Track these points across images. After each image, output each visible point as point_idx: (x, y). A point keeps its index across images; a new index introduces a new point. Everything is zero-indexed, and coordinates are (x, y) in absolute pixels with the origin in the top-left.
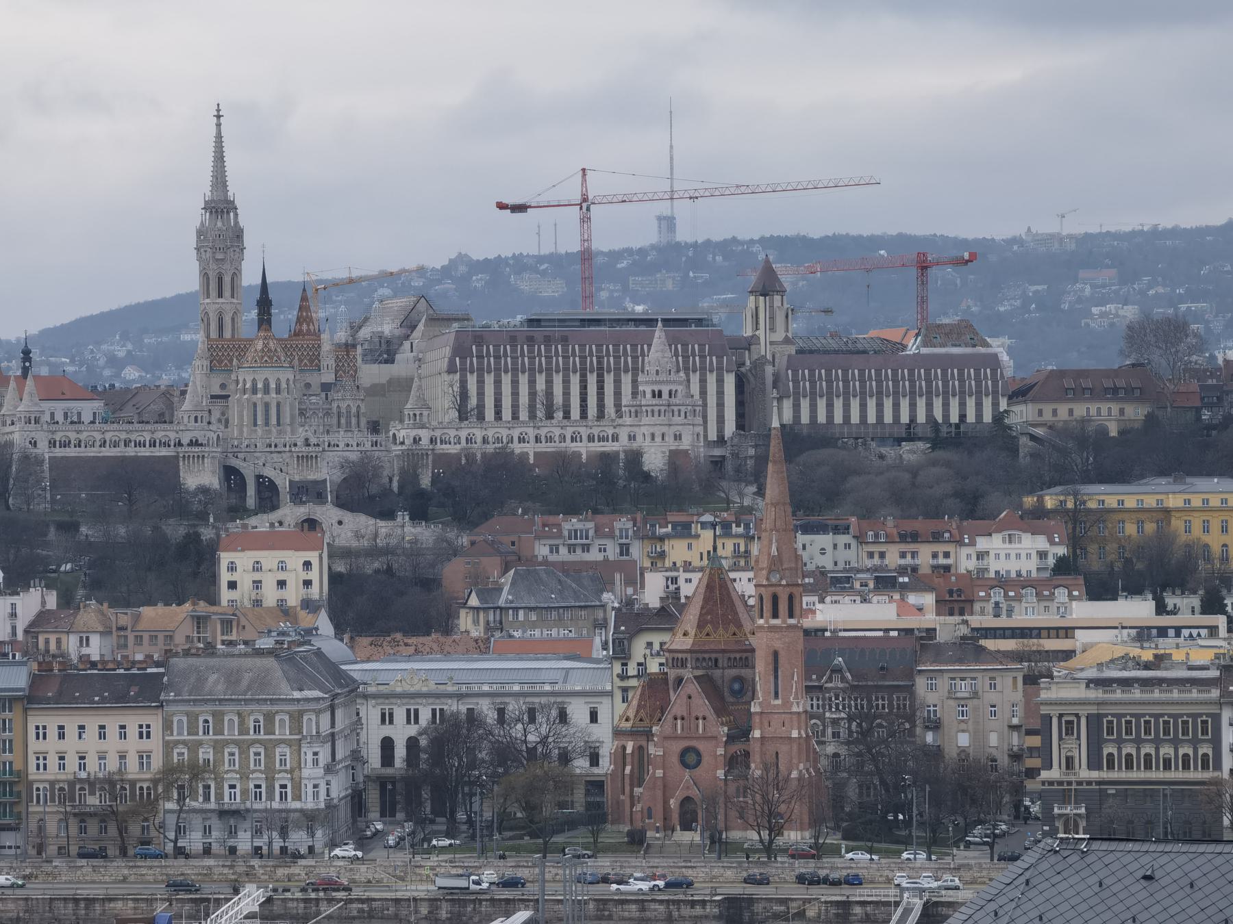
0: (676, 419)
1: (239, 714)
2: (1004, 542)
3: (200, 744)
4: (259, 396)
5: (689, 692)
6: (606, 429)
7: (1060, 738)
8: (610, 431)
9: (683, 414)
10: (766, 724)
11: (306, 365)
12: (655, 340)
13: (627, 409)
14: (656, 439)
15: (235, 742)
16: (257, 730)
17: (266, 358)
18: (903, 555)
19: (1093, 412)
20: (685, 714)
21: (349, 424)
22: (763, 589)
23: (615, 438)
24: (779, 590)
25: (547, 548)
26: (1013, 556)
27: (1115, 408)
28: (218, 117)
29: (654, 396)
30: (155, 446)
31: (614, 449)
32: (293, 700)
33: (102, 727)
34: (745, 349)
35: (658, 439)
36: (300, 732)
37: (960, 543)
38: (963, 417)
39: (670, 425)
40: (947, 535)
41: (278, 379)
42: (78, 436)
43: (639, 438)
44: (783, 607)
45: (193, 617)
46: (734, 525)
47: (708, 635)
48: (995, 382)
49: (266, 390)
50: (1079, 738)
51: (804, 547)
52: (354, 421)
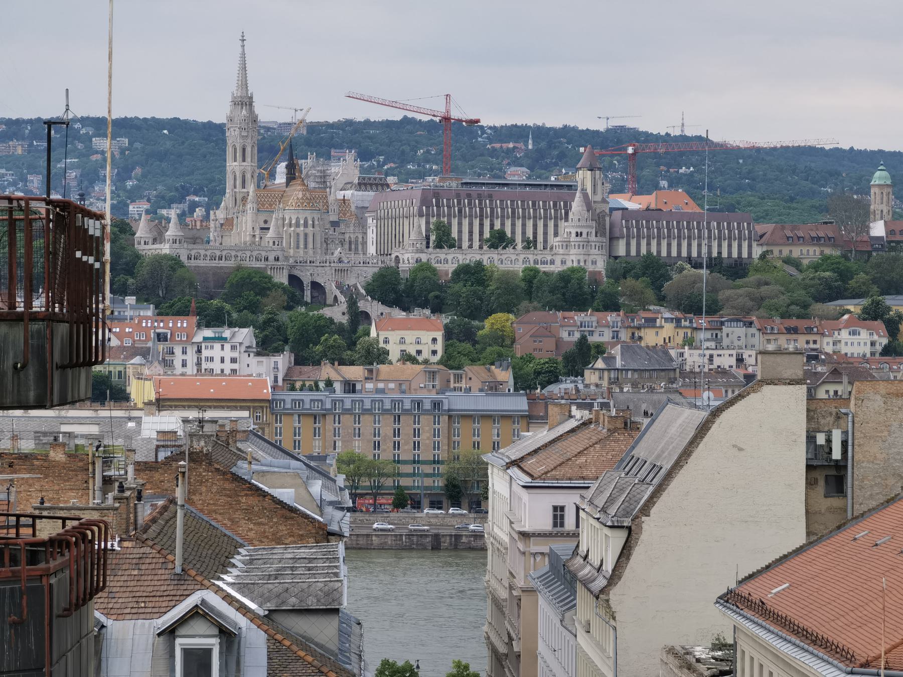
2: (850, 334)
6: (546, 256)
8: (549, 258)
9: (597, 247)
13: (557, 244)
17: (305, 204)
18: (808, 342)
23: (552, 262)
25: (567, 332)
26: (856, 344)
27: (818, 250)
29: (577, 236)
37: (823, 335)
40: (815, 330)
41: (313, 218)
42: (206, 253)
46: (683, 320)
48: (750, 232)
51: (728, 335)
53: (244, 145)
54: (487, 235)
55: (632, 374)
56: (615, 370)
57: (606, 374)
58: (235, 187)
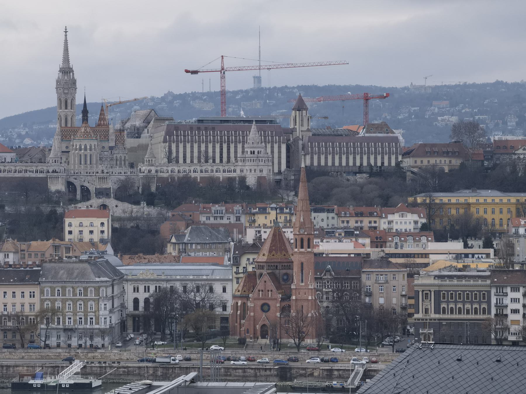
0: (261, 163)
1: (73, 288)
2: (400, 217)
3: (56, 300)
4: (82, 151)
5: (265, 280)
7: (423, 300)
8: (232, 168)
10: (298, 293)
11: (102, 138)
12: (252, 129)
13: (240, 159)
14: (252, 172)
15: (71, 299)
16: (80, 294)
17: (85, 136)
18: (357, 222)
19: (438, 162)
20: (263, 289)
21: (121, 164)
22: (297, 236)
23: (235, 171)
24: (303, 236)
25: (205, 217)
26: (403, 223)
27: (447, 160)
28: (66, 32)
29: (251, 153)
30: (37, 173)
31: (234, 176)
32: (96, 282)
33: (14, 293)
34: (291, 133)
35: (253, 172)
36: (99, 295)
37: (381, 217)
38: (383, 163)
39: (258, 166)
40: (375, 214)
41: (91, 144)
42: (5, 168)
43: (245, 171)
44: (305, 244)
45: (53, 246)
46: (285, 209)
47: (273, 255)
49: (86, 149)
50: (430, 300)
51: (315, 218)
52: (123, 163)
53: (66, 99)
55: (196, 246)
56: (183, 243)
57: (177, 246)
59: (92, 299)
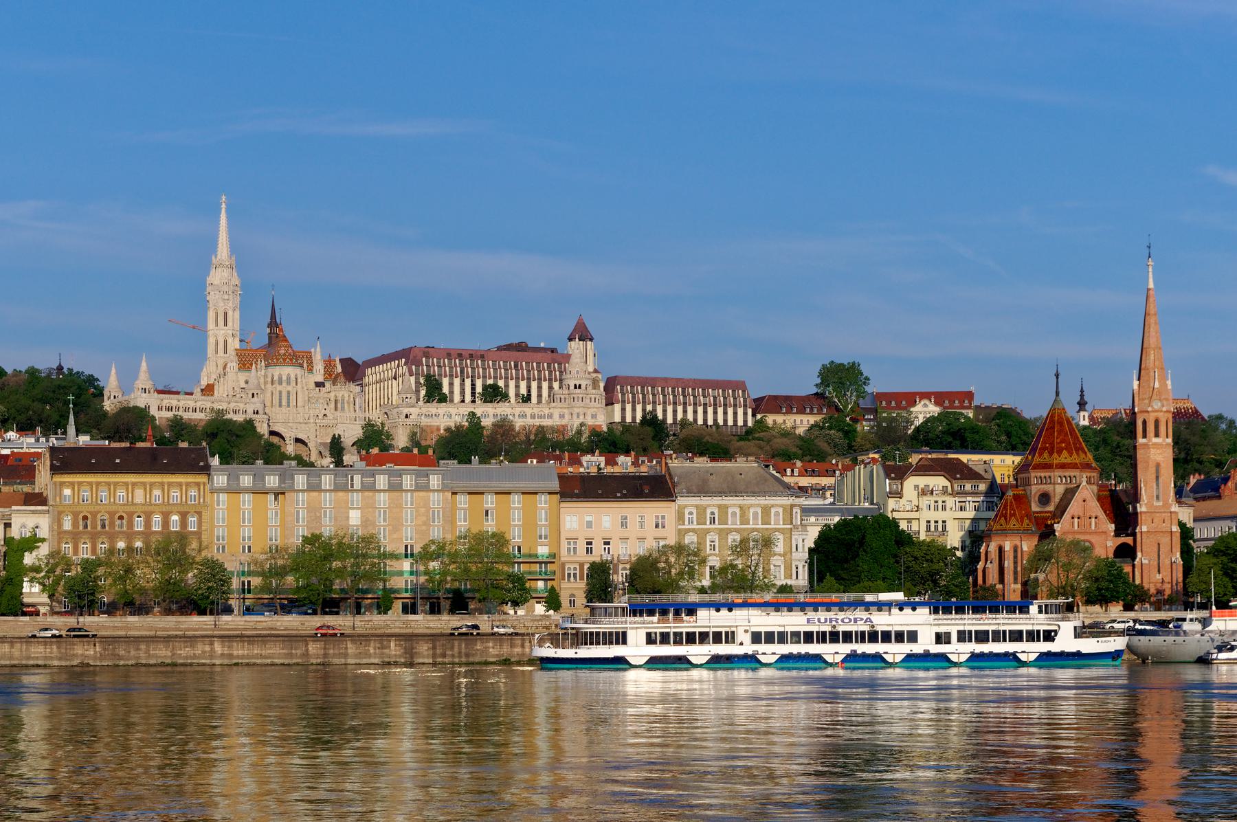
1: (741, 507)
3: (708, 531)
5: (1084, 496)
20: (1081, 514)
23: (550, 416)
36: (791, 523)
41: (296, 375)
54: (479, 389)
58: (217, 352)
59: (779, 529)
